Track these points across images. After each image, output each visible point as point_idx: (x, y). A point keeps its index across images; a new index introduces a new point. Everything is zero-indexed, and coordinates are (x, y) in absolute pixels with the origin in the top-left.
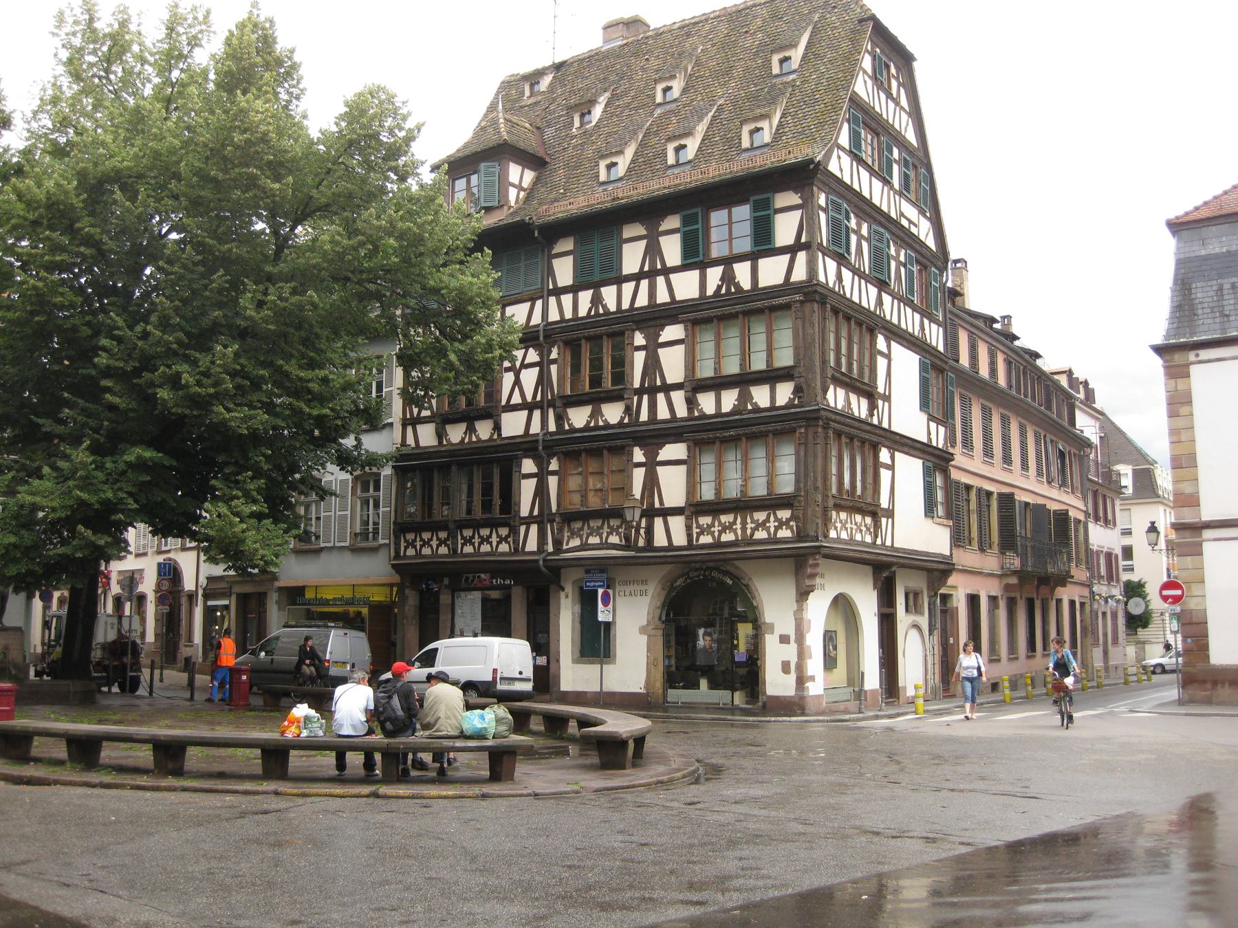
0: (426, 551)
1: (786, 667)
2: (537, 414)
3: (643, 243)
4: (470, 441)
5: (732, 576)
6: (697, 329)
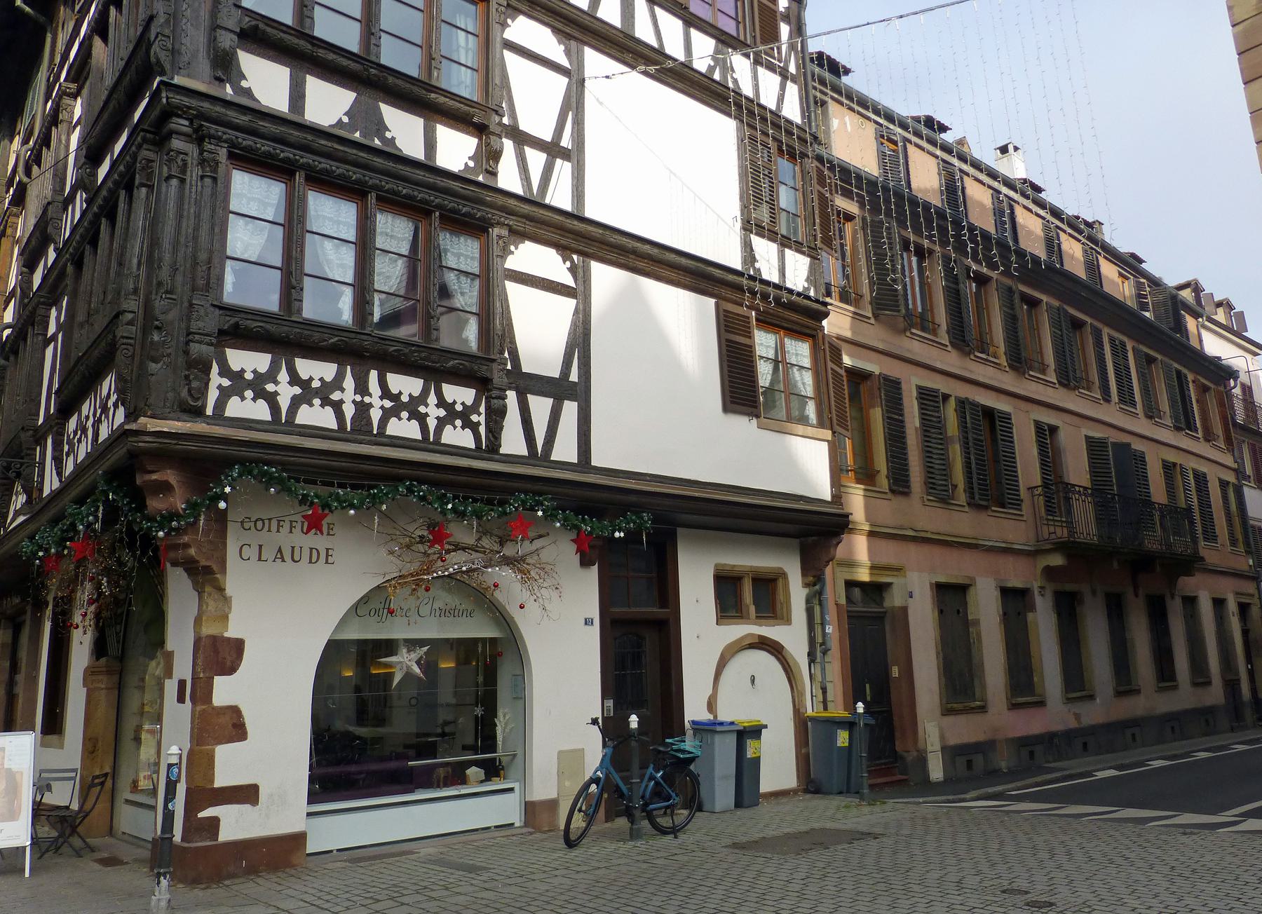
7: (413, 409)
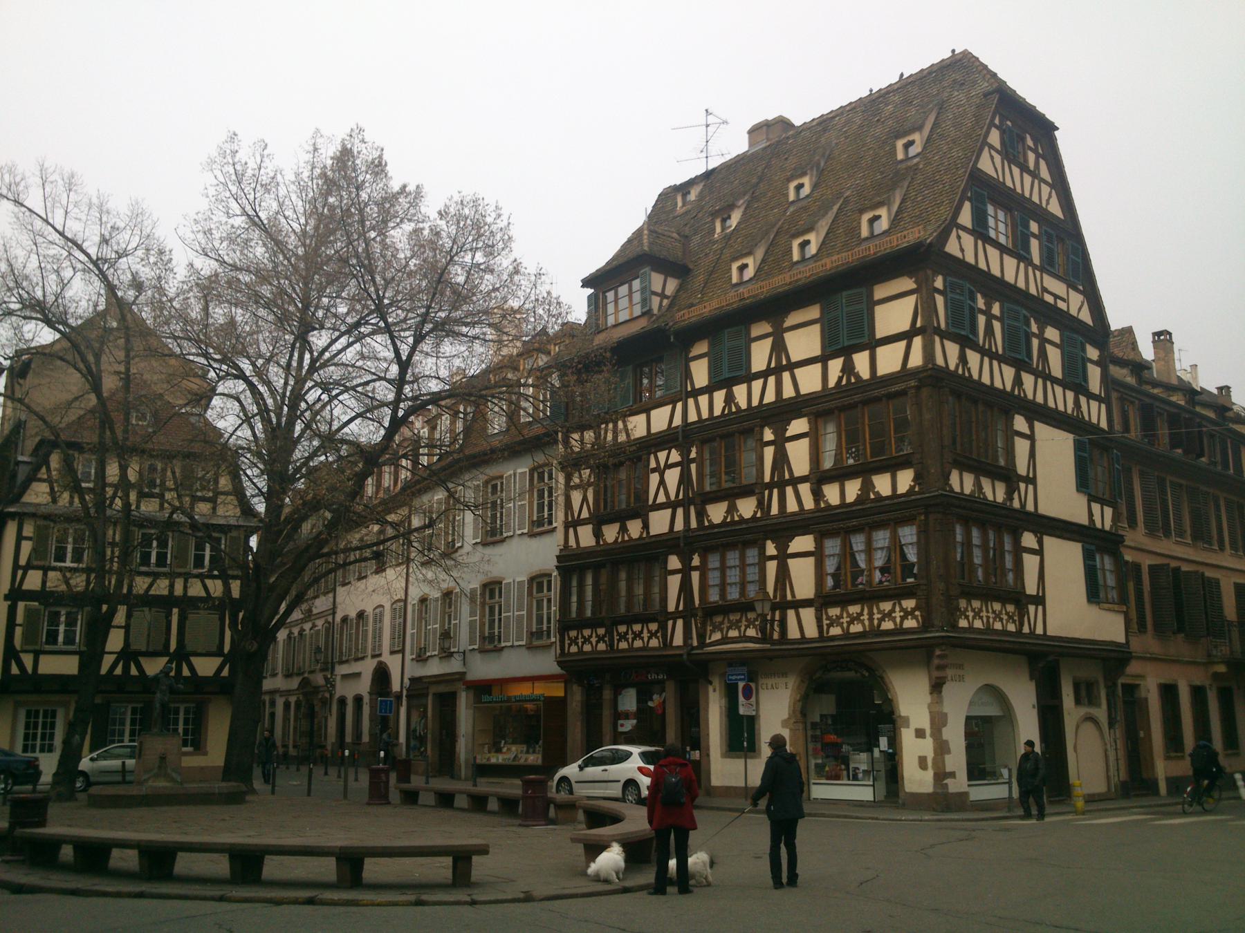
0: (587, 648)
1: (922, 763)
2: (680, 511)
3: (769, 341)
4: (623, 541)
5: (869, 669)
6: (820, 422)
7: (998, 616)
